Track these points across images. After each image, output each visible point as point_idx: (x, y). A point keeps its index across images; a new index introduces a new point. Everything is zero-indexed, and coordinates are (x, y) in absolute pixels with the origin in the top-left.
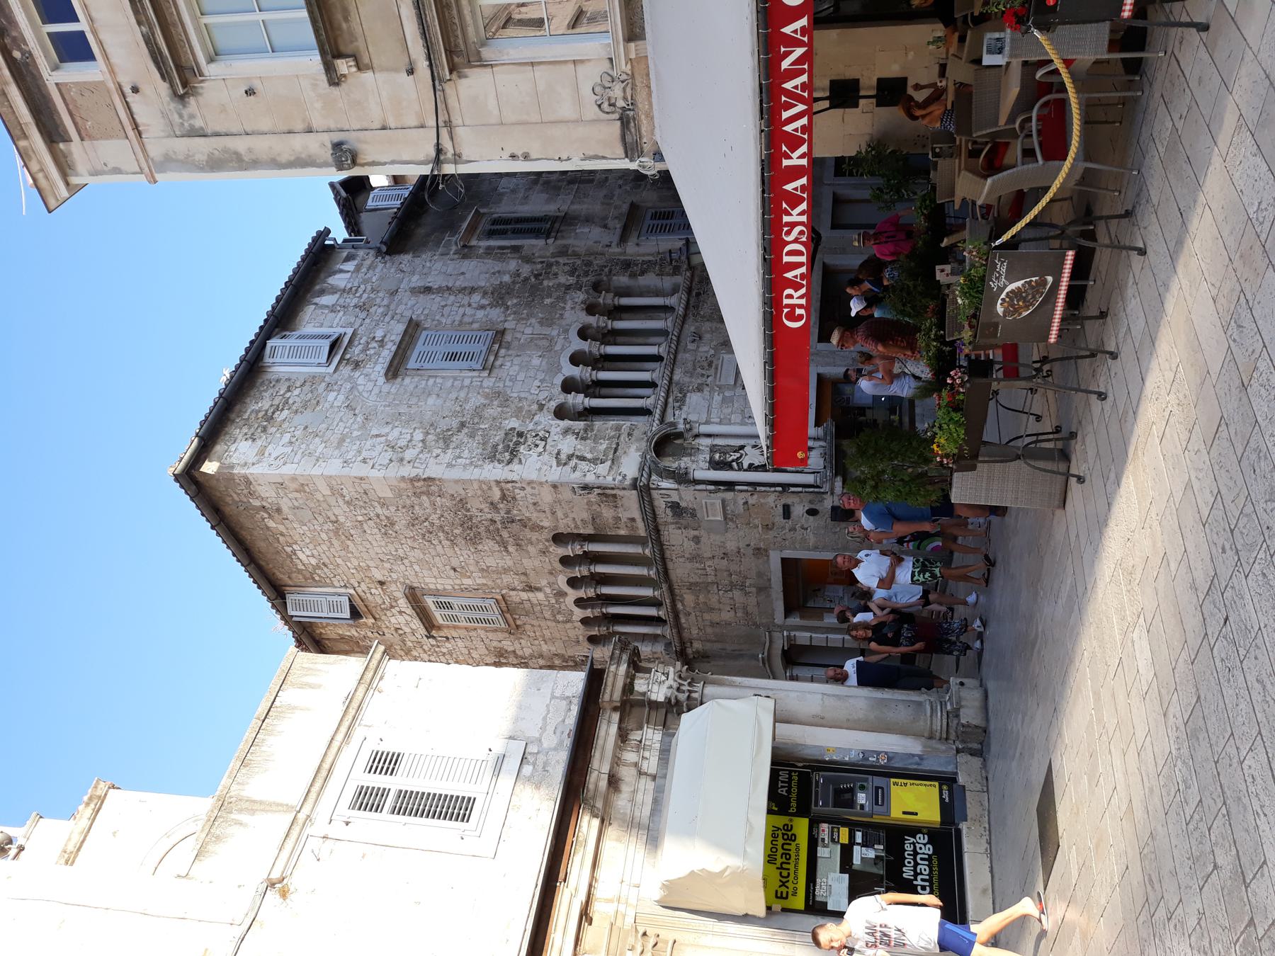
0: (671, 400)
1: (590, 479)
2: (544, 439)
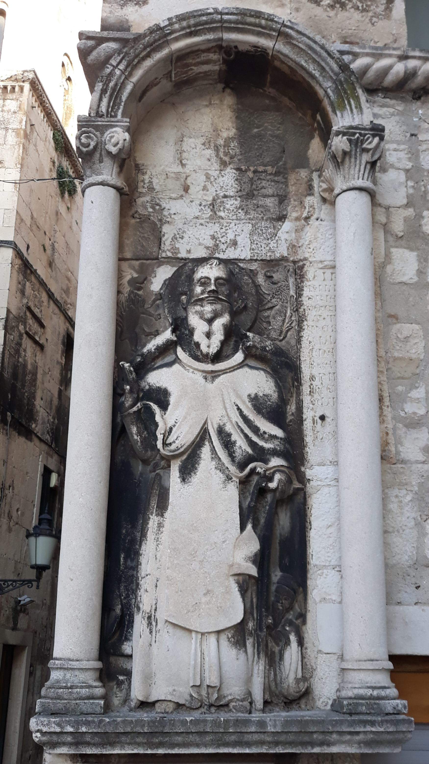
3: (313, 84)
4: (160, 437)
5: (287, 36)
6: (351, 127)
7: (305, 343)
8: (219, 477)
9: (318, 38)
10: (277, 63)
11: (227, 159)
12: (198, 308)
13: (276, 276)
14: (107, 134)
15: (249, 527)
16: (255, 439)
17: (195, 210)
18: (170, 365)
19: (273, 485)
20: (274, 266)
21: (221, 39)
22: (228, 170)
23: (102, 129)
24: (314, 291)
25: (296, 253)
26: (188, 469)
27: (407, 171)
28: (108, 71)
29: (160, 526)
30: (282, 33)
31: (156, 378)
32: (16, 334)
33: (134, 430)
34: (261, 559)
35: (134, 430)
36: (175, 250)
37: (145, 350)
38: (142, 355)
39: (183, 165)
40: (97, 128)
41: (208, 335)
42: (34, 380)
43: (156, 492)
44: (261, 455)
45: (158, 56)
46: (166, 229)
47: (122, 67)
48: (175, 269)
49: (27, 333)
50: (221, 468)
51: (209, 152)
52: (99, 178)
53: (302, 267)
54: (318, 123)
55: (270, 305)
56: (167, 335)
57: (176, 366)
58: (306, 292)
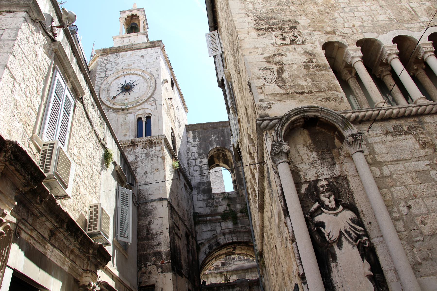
0: (394, 122)
1: (256, 83)
2: (292, 42)
3: (335, 124)
4: (327, 237)
5: (324, 111)
6: (352, 134)
7: (356, 201)
8: (350, 246)
9: (333, 111)
10: (321, 119)
11: (311, 149)
12: (323, 194)
13: (339, 182)
14: (283, 147)
15: (365, 260)
16: (356, 232)
17: (307, 166)
18: (321, 214)
19: (367, 245)
20: (337, 179)
21: (304, 115)
22: (313, 152)
23: (281, 146)
24: (353, 184)
25: (343, 174)
26: (340, 245)
27: (365, 144)
28: (276, 129)
29: (336, 265)
30: (322, 111)
31: (318, 218)
32: (172, 234)
33: (317, 236)
35: (317, 236)
36: (306, 179)
37: (311, 211)
38: (310, 212)
39: (299, 153)
40: (279, 146)
41: (330, 202)
42: (180, 252)
43: (330, 255)
44: (359, 236)
45: (289, 122)
46: (300, 173)
47: (280, 127)
48: (308, 185)
49: (175, 233)
51: (306, 148)
52: (283, 160)
53: (346, 178)
54: (336, 135)
55: (341, 191)
56: (317, 204)
57: (323, 214)
58: (350, 185)
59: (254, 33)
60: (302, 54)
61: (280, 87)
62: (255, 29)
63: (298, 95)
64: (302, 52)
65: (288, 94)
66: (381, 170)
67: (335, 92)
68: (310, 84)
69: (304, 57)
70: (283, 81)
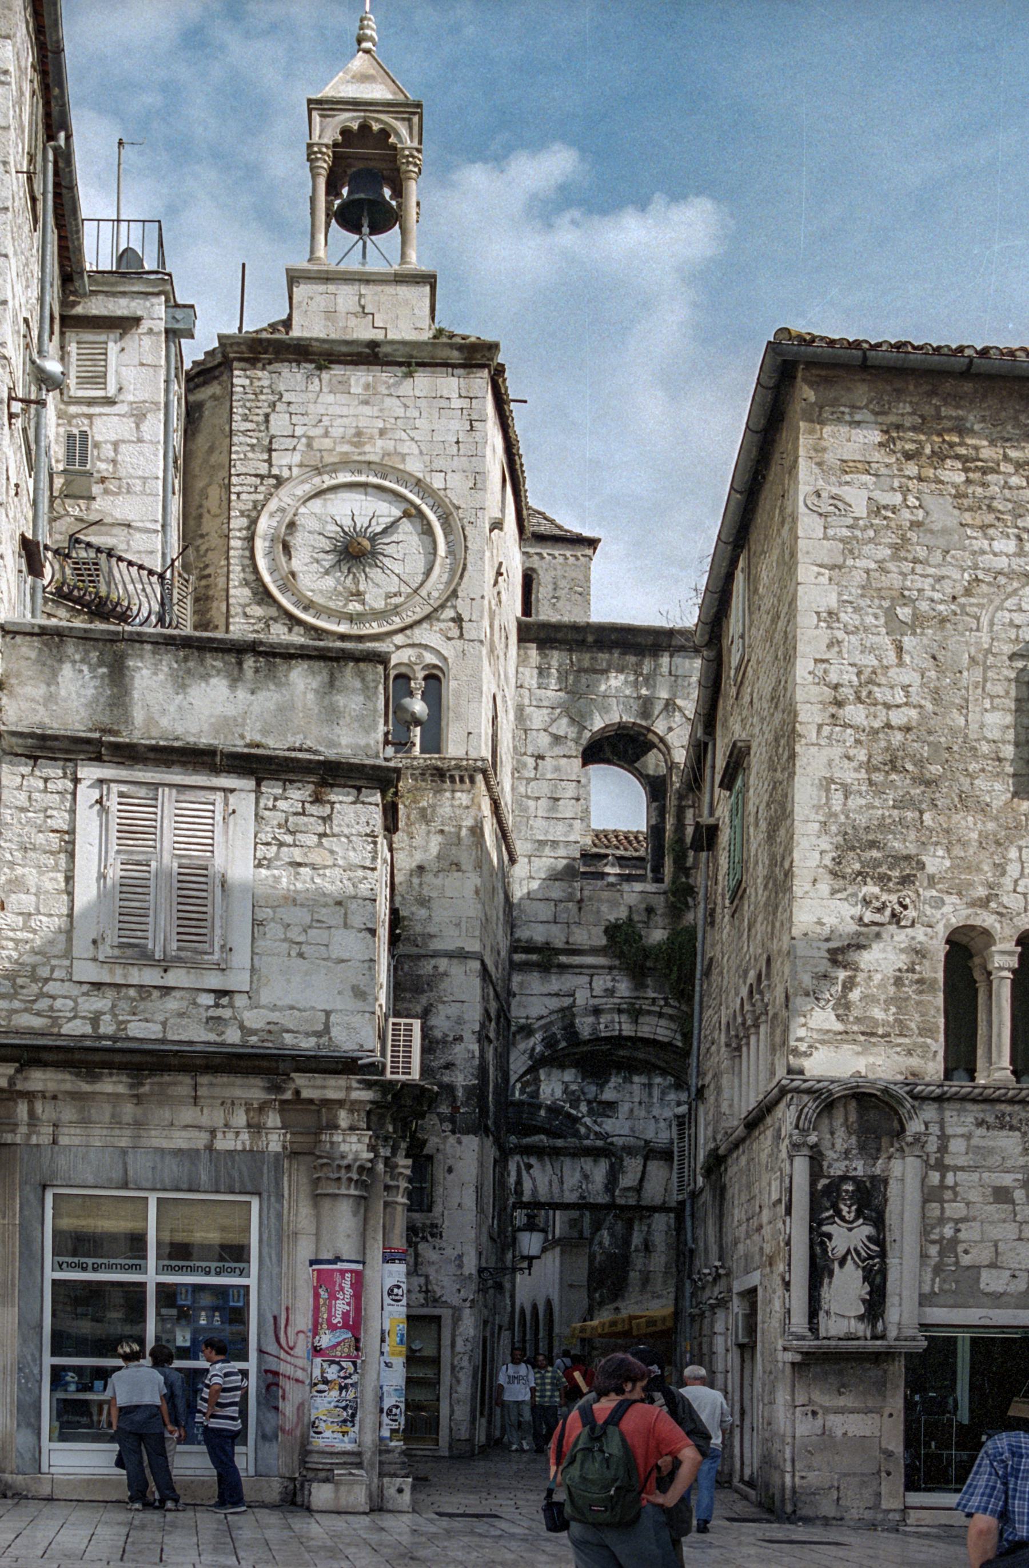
26: (842, 1262)
31: (825, 1229)
34: (870, 1293)
50: (855, 1262)
59: (824, 887)
60: (902, 950)
61: (838, 1016)
62: (831, 872)
63: (862, 1038)
64: (903, 946)
65: (847, 1033)
66: (943, 1177)
67: (929, 1041)
68: (891, 1019)
69: (903, 957)
70: (847, 1006)
